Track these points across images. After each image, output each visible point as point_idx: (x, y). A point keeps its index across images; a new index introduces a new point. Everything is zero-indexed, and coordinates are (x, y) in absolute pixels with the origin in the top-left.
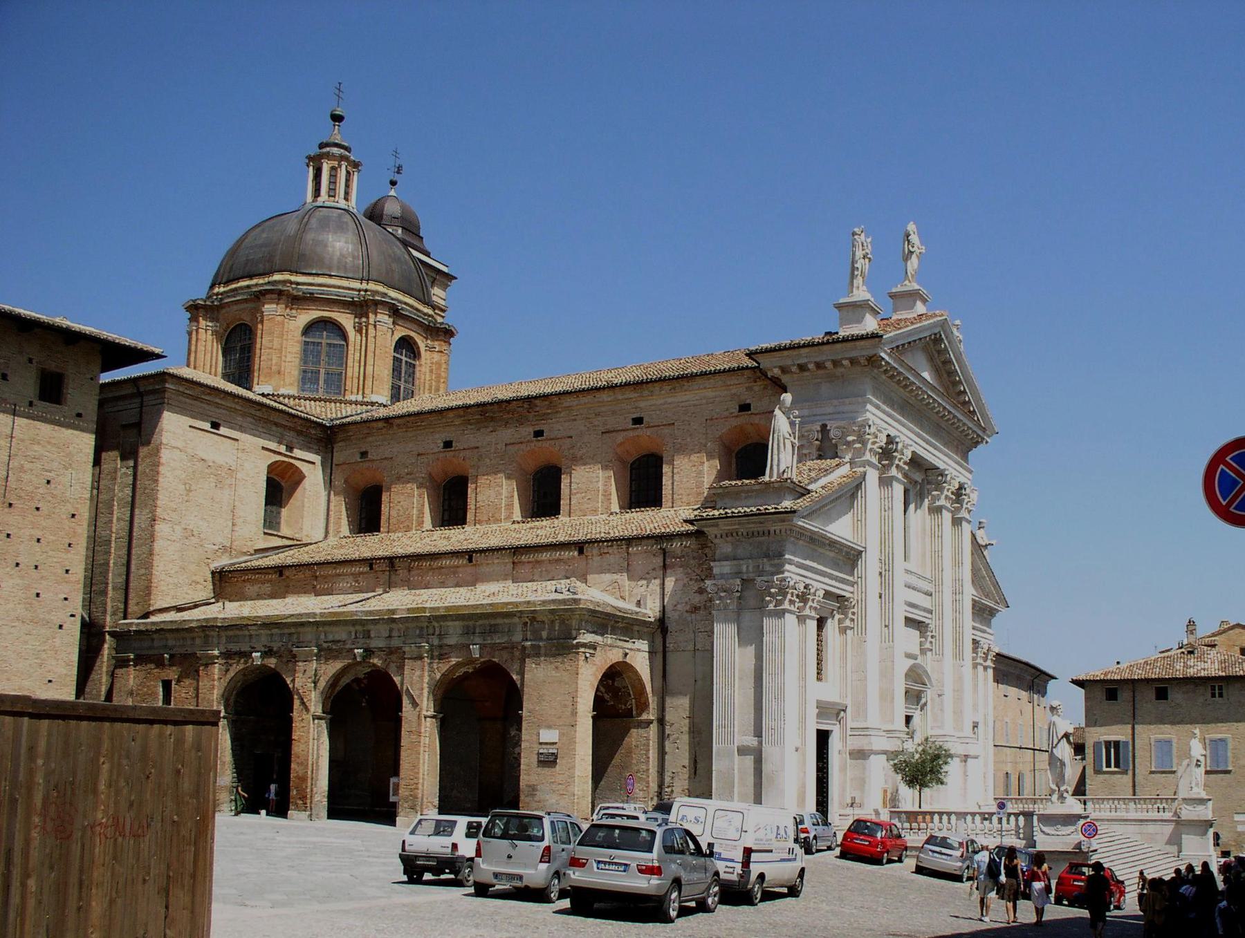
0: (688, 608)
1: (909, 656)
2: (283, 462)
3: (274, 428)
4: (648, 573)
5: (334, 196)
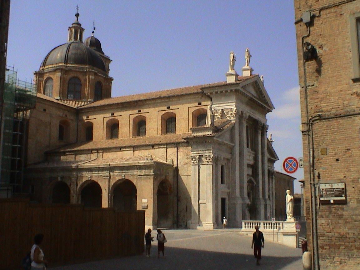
0: (184, 163)
1: (248, 175)
4: (172, 153)
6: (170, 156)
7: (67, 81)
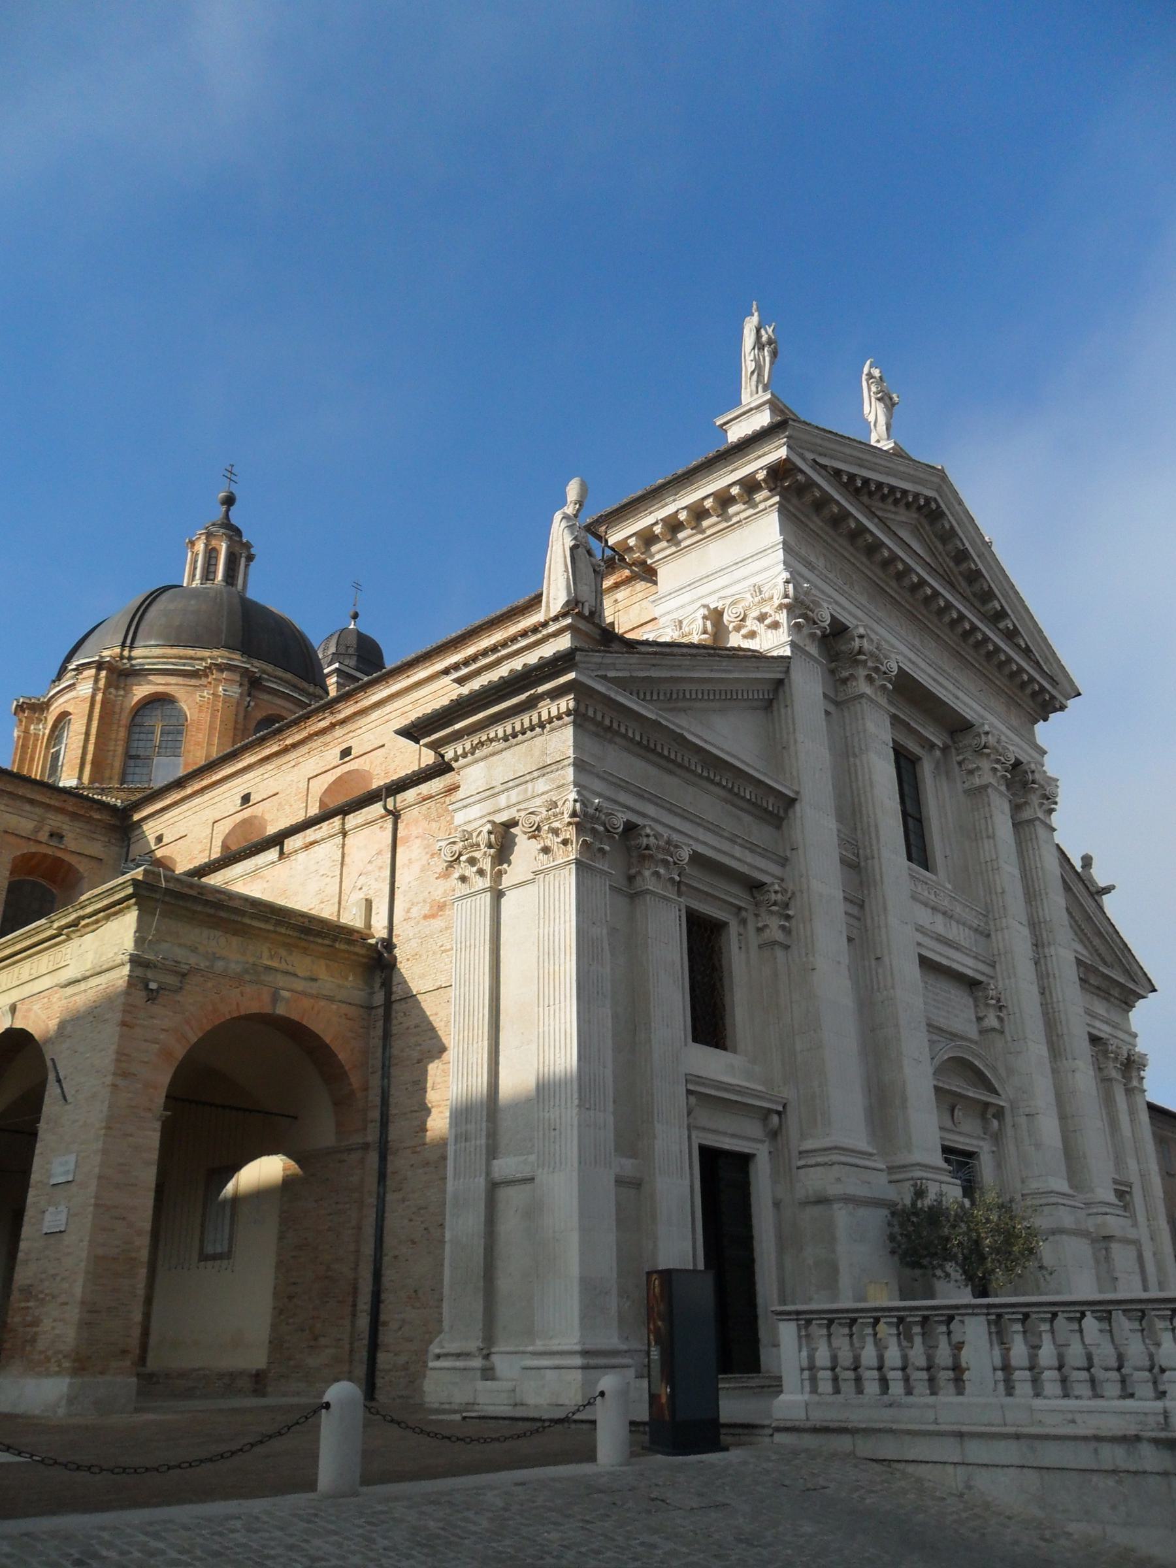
0: (426, 910)
2: (45, 855)
3: (28, 807)
5: (214, 580)
6: (359, 885)
7: (125, 718)
